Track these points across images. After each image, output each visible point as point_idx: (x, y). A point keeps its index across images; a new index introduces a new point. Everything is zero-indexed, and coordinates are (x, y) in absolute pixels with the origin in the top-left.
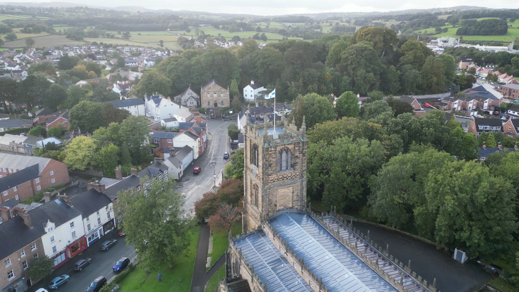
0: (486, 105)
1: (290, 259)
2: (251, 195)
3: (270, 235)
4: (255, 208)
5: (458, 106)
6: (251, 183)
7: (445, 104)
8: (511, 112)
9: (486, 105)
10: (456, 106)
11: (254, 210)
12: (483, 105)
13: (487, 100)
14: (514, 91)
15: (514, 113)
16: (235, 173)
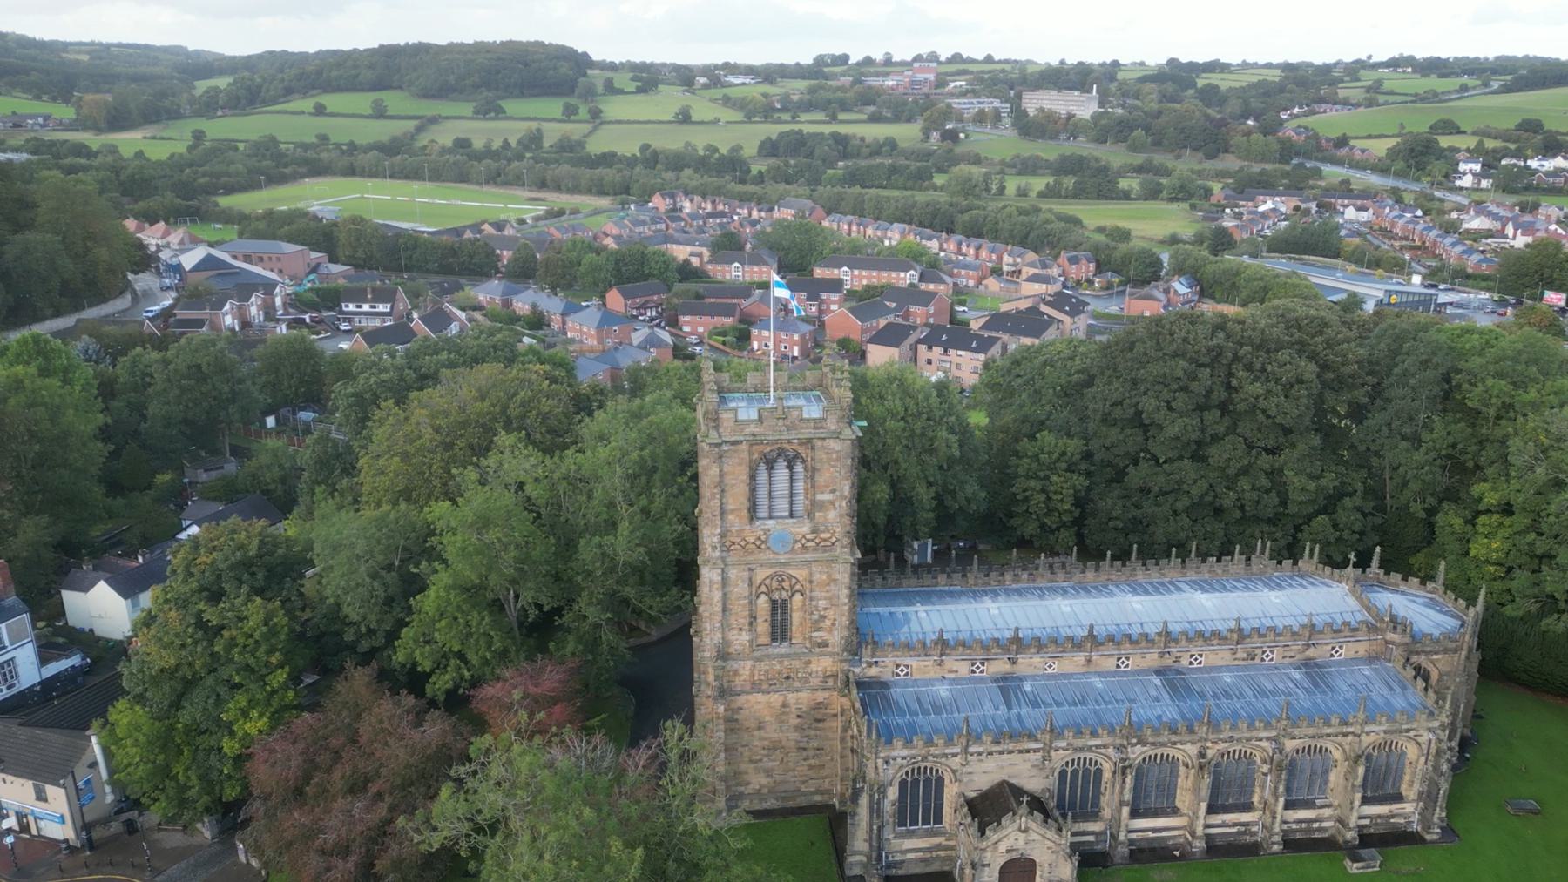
0: (278, 301)
1: (1030, 663)
2: (751, 624)
3: (919, 666)
4: (784, 648)
5: (233, 319)
6: (751, 584)
7: (199, 323)
8: (352, 307)
9: (278, 301)
10: (228, 320)
11: (781, 656)
12: (274, 302)
13: (278, 290)
14: (270, 259)
15: (360, 307)
16: (245, 714)
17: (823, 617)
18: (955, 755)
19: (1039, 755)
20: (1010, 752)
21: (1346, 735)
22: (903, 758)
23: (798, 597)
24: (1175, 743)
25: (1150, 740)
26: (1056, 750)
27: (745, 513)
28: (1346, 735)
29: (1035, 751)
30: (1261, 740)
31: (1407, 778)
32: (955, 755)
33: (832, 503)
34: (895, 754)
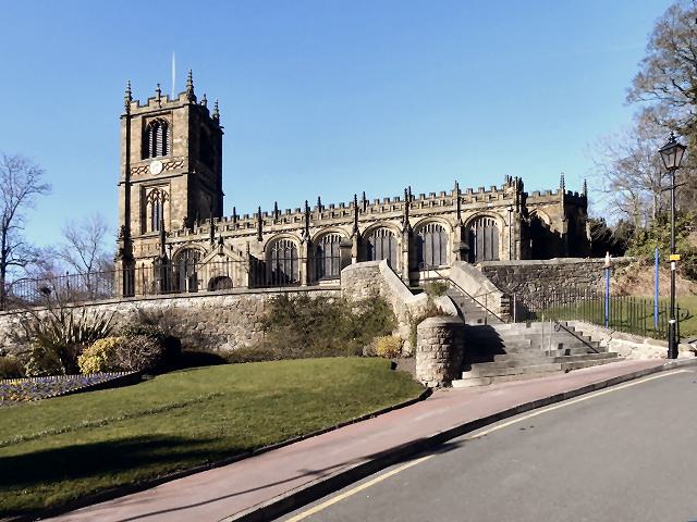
17: (176, 211)
18: (207, 240)
19: (257, 236)
20: (238, 236)
21: (450, 212)
22: (179, 243)
23: (167, 203)
24: (337, 225)
25: (323, 223)
26: (265, 233)
27: (139, 154)
28: (450, 212)
29: (253, 234)
30: (392, 219)
31: (500, 246)
32: (207, 240)
33: (180, 143)
34: (174, 240)
